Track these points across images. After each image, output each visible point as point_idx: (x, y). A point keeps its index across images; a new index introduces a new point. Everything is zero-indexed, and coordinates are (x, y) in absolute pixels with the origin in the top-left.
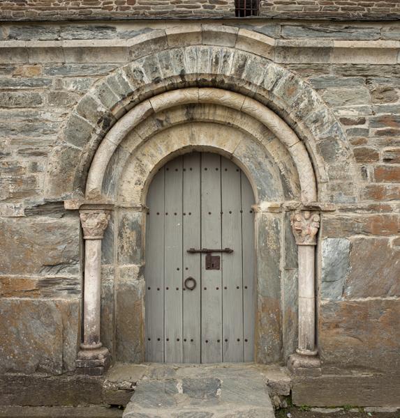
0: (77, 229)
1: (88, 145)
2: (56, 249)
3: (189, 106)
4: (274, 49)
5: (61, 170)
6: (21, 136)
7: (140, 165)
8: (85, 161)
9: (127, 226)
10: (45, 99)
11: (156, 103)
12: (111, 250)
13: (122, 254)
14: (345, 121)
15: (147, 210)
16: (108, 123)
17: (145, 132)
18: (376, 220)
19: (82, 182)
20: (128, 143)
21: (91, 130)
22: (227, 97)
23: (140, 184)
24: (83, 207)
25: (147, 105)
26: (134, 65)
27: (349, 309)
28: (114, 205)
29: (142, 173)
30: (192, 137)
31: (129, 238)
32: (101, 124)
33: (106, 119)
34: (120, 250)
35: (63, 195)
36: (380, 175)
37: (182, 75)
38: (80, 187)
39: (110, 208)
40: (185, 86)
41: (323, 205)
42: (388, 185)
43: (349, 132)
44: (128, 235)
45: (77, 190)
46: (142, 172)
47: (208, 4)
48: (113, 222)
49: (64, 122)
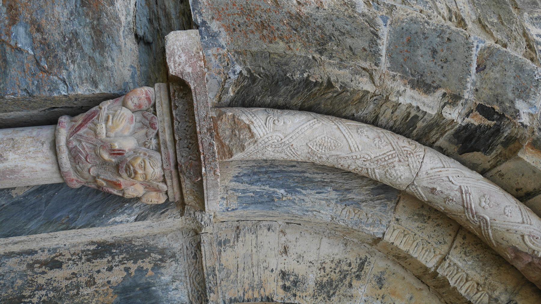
0: (95, 84)
1: (399, 85)
2: (13, 21)
5: (298, 17)
7: (344, 275)
8: (344, 87)
9: (134, 267)
12: (32, 225)
13: (31, 266)
20: (413, 225)
21: (453, 89)
23: (285, 288)
28: (203, 210)
29: (320, 286)
31: (91, 282)
32: (476, 120)
33: (498, 130)
34: (43, 257)
35: (214, 26)
38: (253, 79)
39: (189, 199)
44: (100, 279)
45: (238, 68)
48: (140, 218)
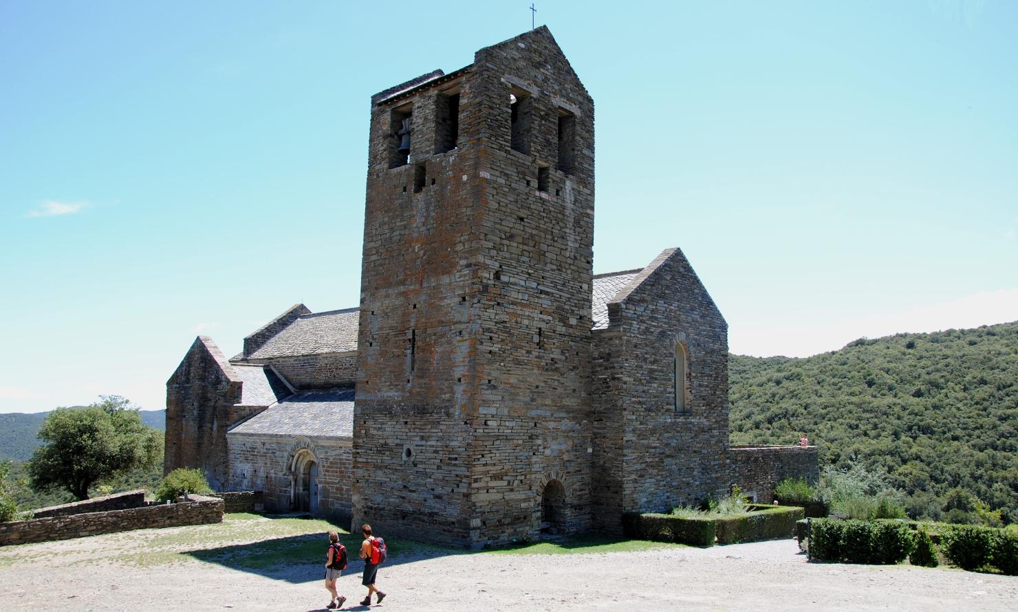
16: (293, 456)
17: (301, 457)
19: (290, 469)
42: (327, 473)
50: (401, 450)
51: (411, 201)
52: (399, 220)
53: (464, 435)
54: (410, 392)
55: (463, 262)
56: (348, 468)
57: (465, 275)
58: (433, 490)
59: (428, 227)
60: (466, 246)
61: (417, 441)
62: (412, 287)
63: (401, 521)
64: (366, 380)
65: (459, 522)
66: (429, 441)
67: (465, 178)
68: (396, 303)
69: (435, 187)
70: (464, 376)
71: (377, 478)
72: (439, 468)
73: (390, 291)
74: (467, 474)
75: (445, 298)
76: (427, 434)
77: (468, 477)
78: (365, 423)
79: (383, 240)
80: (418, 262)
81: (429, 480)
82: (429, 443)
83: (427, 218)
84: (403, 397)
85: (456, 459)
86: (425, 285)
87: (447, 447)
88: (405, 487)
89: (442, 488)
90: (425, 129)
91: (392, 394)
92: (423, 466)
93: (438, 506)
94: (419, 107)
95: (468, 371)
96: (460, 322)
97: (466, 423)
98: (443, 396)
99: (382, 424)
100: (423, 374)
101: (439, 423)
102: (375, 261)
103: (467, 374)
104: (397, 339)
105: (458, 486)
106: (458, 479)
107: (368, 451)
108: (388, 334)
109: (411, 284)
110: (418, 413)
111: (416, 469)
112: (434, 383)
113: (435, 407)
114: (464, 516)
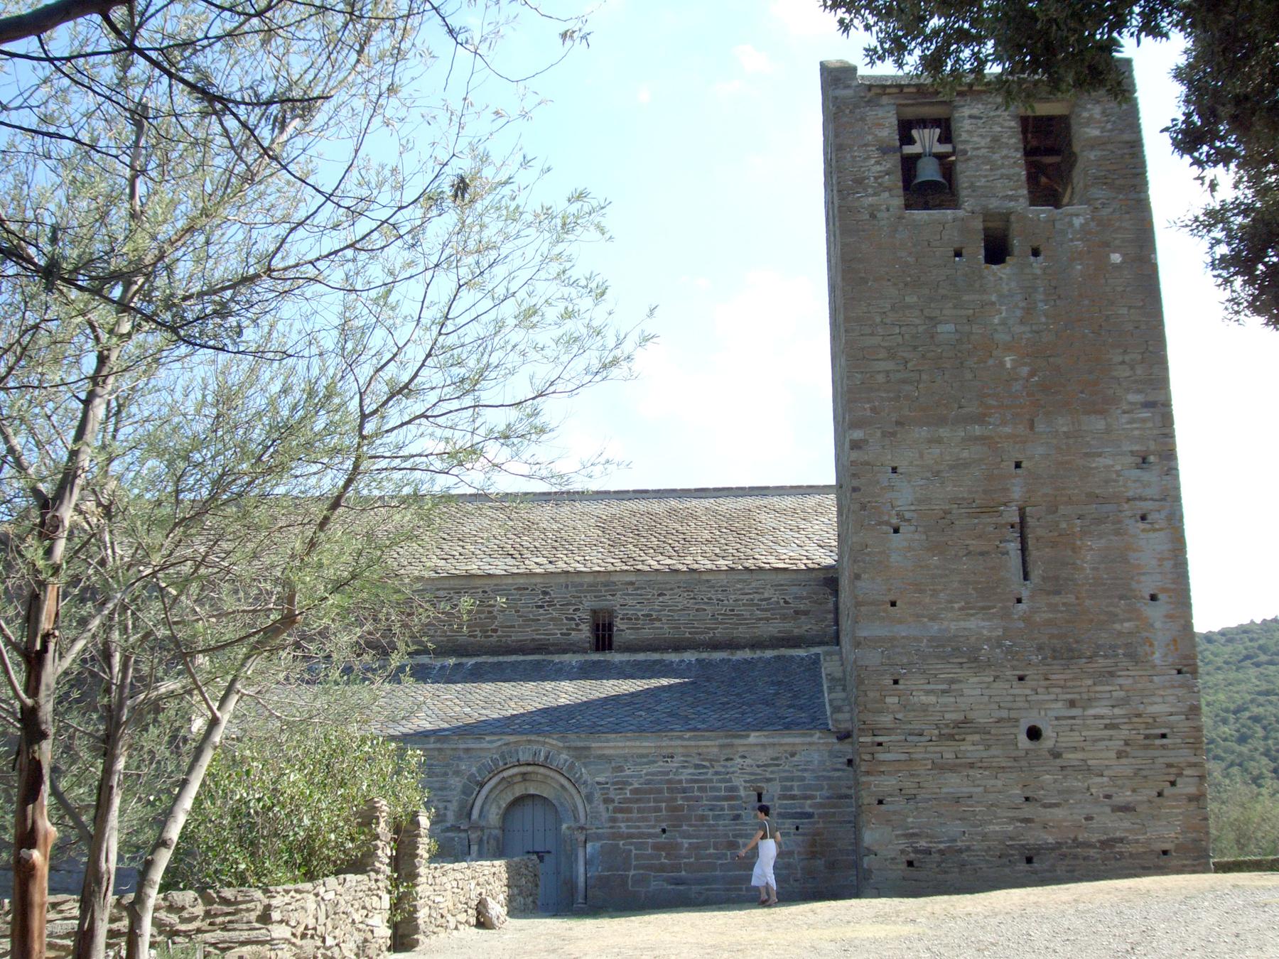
3: (524, 774)
4: (564, 747)
6: (440, 793)
10: (450, 773)
11: (505, 774)
14: (598, 783)
15: (503, 829)
16: (482, 786)
17: (501, 787)
18: (614, 833)
19: (469, 815)
22: (542, 770)
24: (469, 828)
25: (501, 775)
26: (495, 756)
27: (600, 878)
30: (526, 789)
36: (616, 810)
37: (518, 761)
40: (520, 765)
41: (587, 827)
42: (619, 815)
43: (601, 789)
46: (500, 808)
47: (565, 631)
49: (460, 785)
50: (1014, 730)
51: (982, 277)
52: (950, 305)
53: (1181, 692)
54: (1027, 619)
55: (1132, 397)
56: (698, 799)
57: (1144, 420)
58: (1108, 797)
59: (1034, 328)
60: (1139, 372)
61: (1059, 708)
62: (1008, 430)
63: (1023, 866)
64: (892, 598)
65: (1179, 848)
66: (1091, 707)
67: (1116, 258)
68: (965, 454)
69: (1038, 264)
70: (1164, 590)
71: (944, 790)
72: (1120, 755)
73: (944, 432)
74: (1194, 759)
75: (1100, 455)
76: (1085, 696)
77: (1195, 765)
78: (896, 682)
79: (907, 337)
80: (1017, 386)
81: (1098, 780)
82: (1091, 712)
83: (1030, 310)
84: (1005, 629)
85: (1164, 736)
86: (1040, 427)
87: (1139, 716)
88: (1027, 799)
89: (1134, 791)
90: (996, 157)
91: (977, 626)
92: (1080, 755)
93: (1126, 824)
94: (971, 117)
95: (1173, 583)
96: (1141, 499)
97: (1179, 672)
98: (1117, 626)
99: (952, 681)
100: (1055, 586)
101: (1112, 674)
102: (887, 372)
103: (1173, 586)
104: (976, 521)
105: (1173, 784)
106: (1173, 770)
107: (909, 738)
108: (947, 512)
109: (1004, 423)
110: (1054, 658)
111: (1058, 762)
112: (1088, 603)
113: (1099, 647)
114: (1194, 835)
